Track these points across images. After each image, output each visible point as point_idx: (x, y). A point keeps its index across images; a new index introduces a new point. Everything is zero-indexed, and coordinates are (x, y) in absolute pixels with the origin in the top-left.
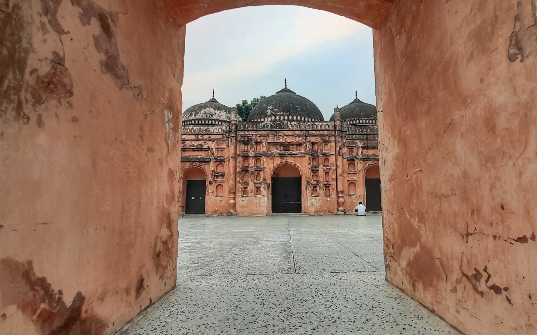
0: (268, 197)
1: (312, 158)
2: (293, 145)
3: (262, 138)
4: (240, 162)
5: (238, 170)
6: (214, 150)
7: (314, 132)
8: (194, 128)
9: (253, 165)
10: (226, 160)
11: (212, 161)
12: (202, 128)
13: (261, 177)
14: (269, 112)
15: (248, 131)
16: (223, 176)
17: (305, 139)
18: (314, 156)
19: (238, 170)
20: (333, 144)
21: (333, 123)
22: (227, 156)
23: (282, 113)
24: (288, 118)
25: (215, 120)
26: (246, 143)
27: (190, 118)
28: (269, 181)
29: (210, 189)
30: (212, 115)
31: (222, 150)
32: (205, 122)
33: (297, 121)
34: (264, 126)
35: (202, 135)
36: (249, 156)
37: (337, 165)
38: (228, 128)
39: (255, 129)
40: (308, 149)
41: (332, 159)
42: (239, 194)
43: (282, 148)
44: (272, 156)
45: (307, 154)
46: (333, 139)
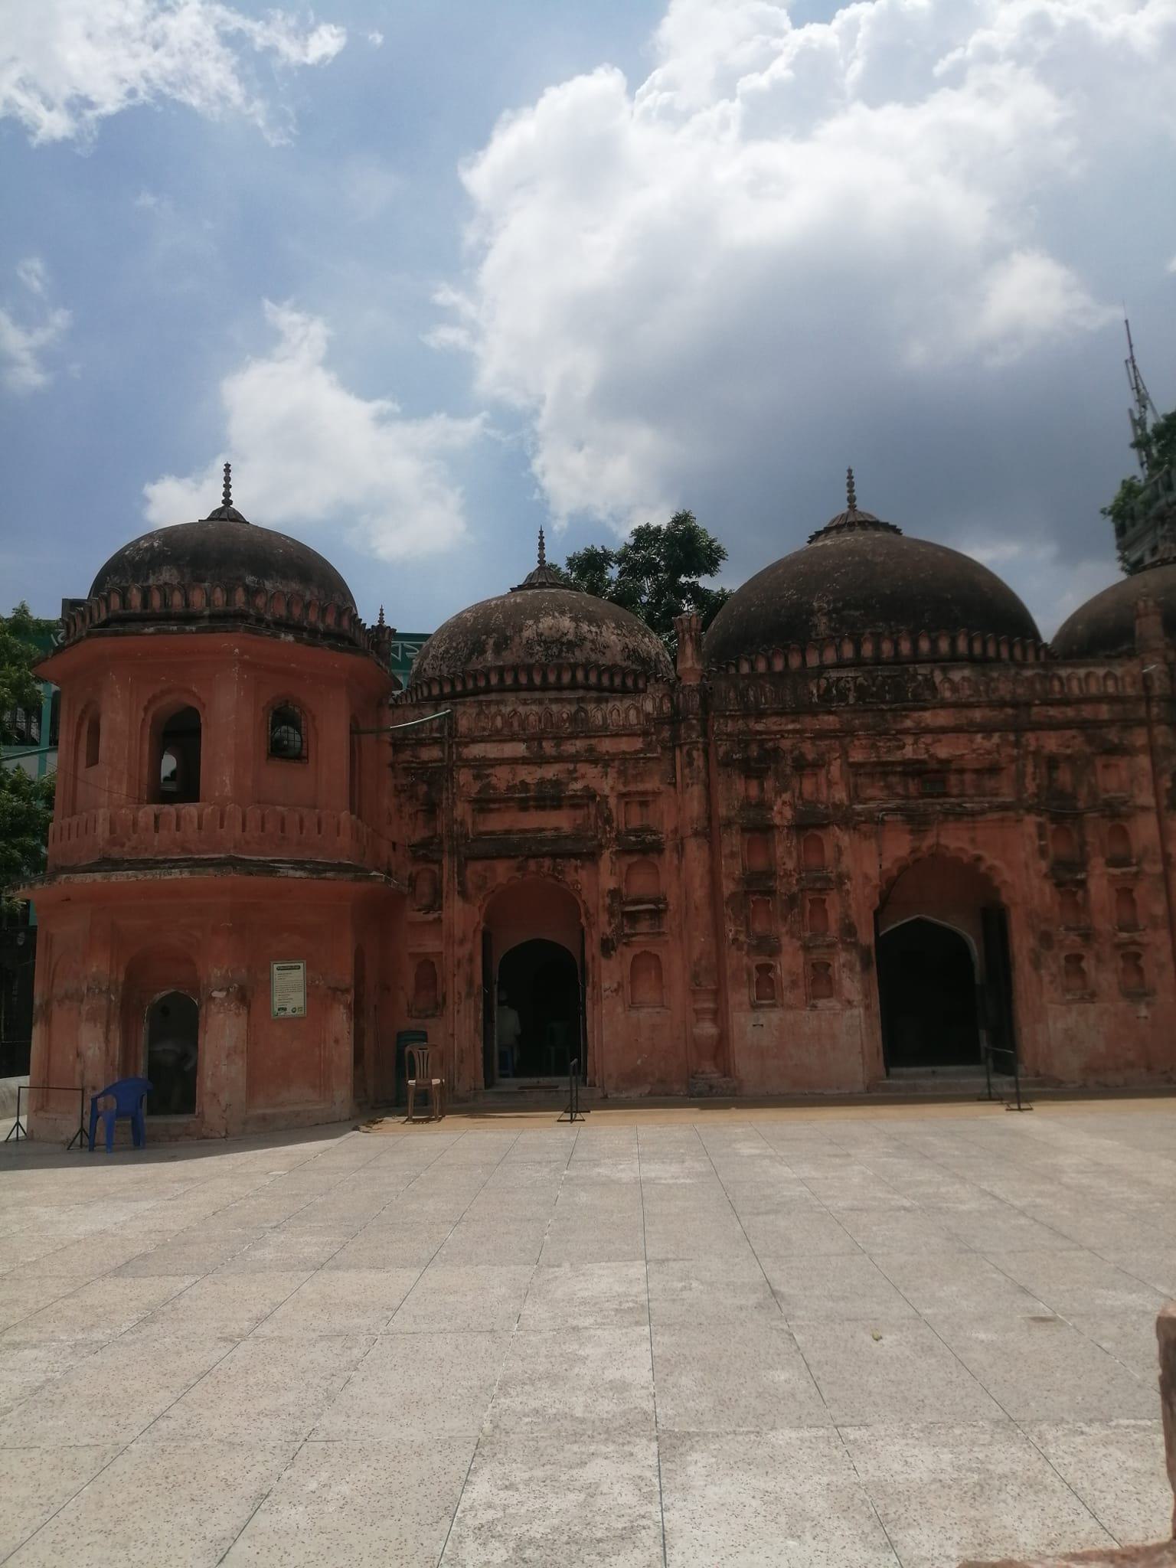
0: (867, 1007)
1: (1051, 827)
3: (823, 744)
4: (733, 855)
5: (728, 887)
7: (1052, 712)
8: (521, 709)
9: (790, 865)
10: (669, 845)
11: (607, 853)
12: (555, 708)
13: (834, 916)
15: (761, 715)
16: (657, 914)
17: (1017, 744)
19: (728, 887)
20: (1144, 761)
22: (668, 825)
25: (587, 667)
27: (476, 664)
28: (867, 937)
29: (608, 975)
30: (571, 645)
31: (645, 801)
34: (828, 690)
35: (559, 740)
36: (770, 828)
38: (667, 707)
40: (1031, 787)
43: (913, 786)
45: (1029, 810)
46: (1139, 737)
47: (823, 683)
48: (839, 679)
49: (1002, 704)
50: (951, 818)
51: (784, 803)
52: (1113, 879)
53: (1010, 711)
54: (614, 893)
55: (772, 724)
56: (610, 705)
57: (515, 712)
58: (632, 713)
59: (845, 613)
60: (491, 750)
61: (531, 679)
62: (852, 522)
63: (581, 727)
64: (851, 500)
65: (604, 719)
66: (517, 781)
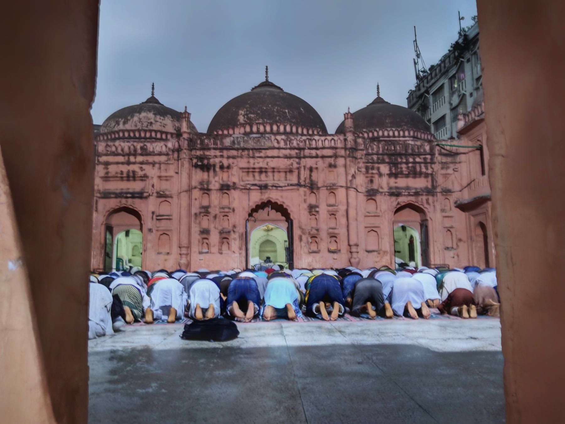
2: (279, 172)
3: (231, 161)
5: (194, 210)
6: (155, 181)
11: (151, 197)
12: (135, 144)
14: (241, 119)
15: (209, 149)
18: (313, 187)
21: (342, 137)
23: (261, 121)
24: (272, 129)
25: (156, 132)
26: (206, 167)
27: (116, 129)
30: (151, 123)
31: (167, 178)
32: (140, 134)
33: (285, 133)
36: (209, 190)
37: (348, 203)
38: (177, 145)
39: (219, 146)
41: (341, 193)
42: (195, 248)
44: (247, 189)
47: (232, 139)
48: (237, 138)
49: (294, 148)
50: (274, 188)
51: (216, 181)
52: (328, 211)
53: (297, 151)
54: (153, 213)
55: (212, 153)
56: (156, 144)
57: (120, 145)
58: (164, 148)
59: (249, 115)
60: (111, 159)
61: (135, 135)
62: (267, 84)
63: (145, 152)
64: (267, 77)
65: (153, 148)
66: (119, 171)
